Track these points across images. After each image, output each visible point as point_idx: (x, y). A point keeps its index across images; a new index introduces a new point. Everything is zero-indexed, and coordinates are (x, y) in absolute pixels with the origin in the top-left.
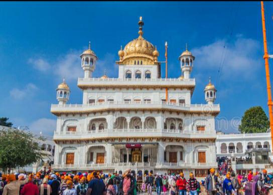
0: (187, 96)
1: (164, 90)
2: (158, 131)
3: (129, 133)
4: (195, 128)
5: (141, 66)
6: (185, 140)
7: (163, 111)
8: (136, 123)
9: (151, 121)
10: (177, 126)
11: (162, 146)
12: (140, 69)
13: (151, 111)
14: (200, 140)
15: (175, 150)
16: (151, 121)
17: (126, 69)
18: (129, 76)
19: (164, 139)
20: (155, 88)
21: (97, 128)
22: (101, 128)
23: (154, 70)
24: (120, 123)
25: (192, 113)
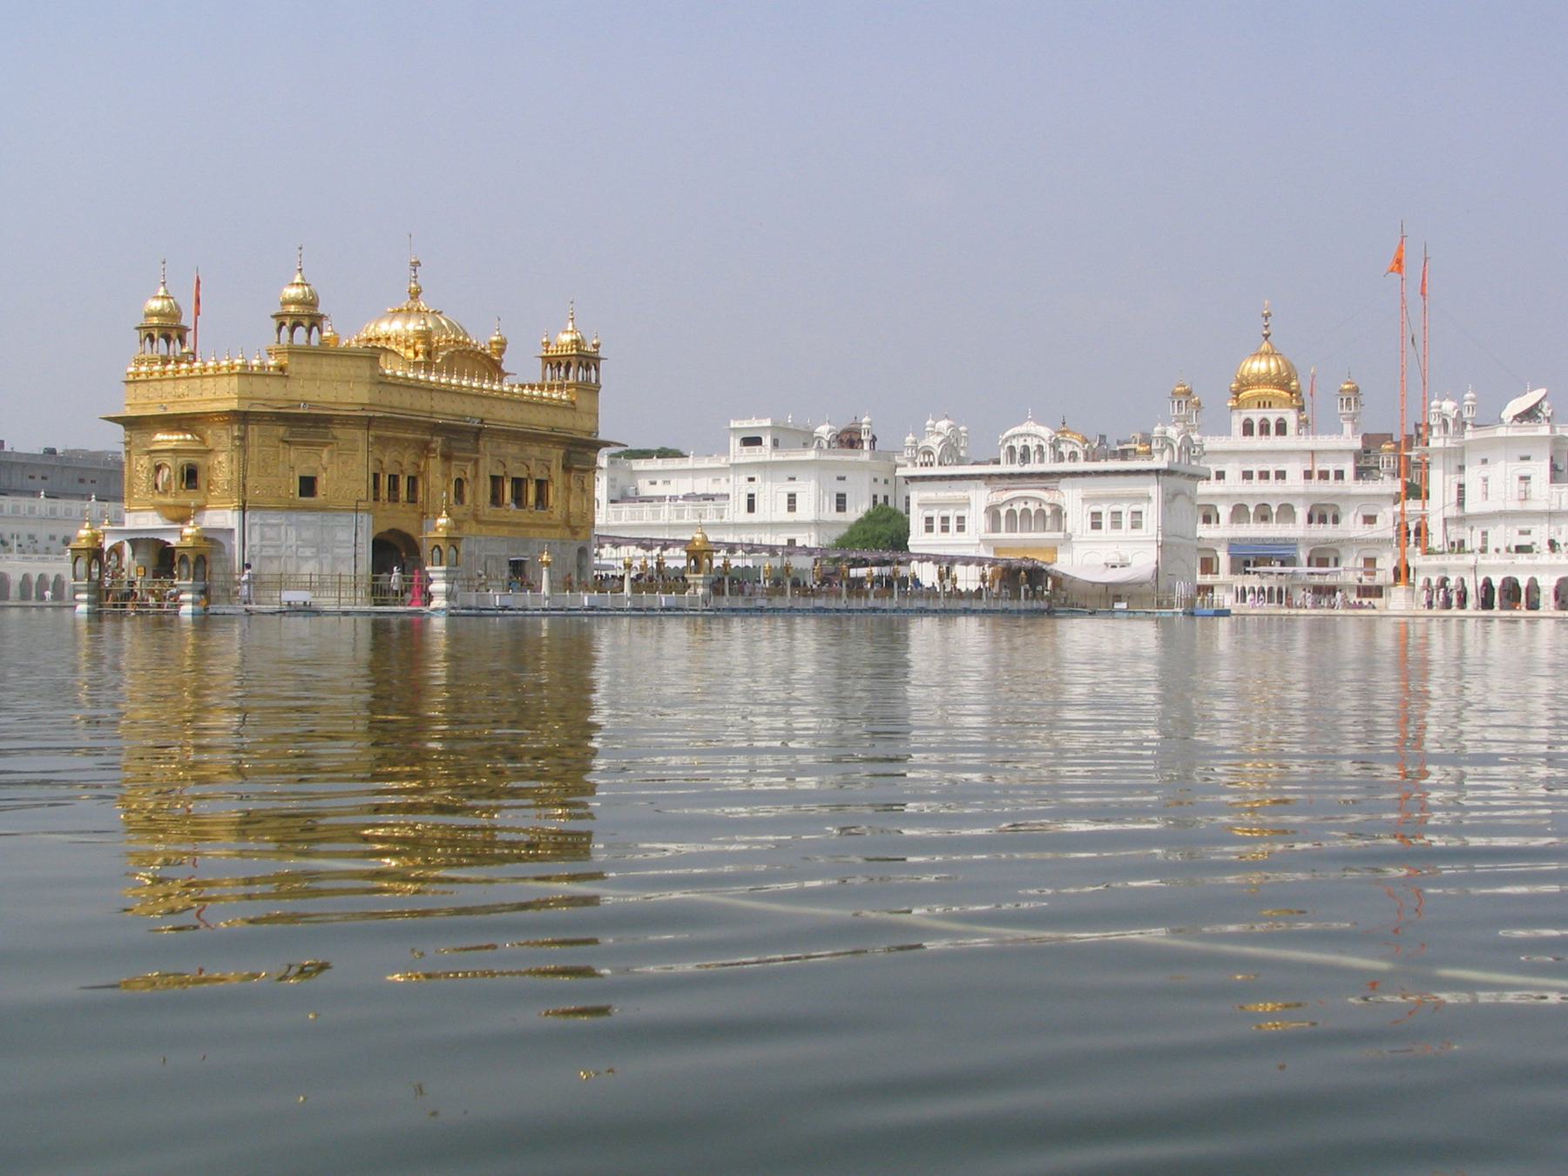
2: (1298, 529)
3: (1253, 530)
5: (1269, 410)
8: (1264, 515)
10: (1330, 518)
12: (1267, 416)
16: (1287, 512)
17: (1244, 417)
18: (1248, 429)
20: (1292, 452)
23: (1291, 418)
24: (1239, 513)
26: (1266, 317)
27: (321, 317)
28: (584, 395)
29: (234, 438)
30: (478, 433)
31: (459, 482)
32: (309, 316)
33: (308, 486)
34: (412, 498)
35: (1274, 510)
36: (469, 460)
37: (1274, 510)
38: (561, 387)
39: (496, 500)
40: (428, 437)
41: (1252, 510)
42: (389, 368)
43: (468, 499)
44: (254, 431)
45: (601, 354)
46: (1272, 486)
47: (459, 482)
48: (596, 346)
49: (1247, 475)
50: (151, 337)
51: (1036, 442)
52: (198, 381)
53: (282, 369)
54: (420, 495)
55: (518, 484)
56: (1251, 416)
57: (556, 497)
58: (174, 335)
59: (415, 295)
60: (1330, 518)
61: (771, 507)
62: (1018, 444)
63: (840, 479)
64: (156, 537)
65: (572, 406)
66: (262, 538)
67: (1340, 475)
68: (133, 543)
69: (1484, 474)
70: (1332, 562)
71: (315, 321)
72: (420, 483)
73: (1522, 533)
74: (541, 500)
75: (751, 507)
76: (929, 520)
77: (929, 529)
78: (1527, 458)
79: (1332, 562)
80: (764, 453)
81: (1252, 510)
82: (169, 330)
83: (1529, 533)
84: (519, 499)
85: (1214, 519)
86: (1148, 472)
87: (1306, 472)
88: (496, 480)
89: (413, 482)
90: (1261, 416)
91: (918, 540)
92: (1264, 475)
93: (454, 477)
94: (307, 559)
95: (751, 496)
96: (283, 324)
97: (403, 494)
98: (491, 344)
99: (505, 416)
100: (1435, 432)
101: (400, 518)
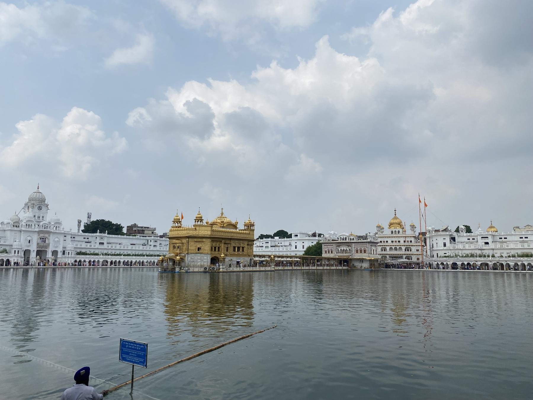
0: (413, 239)
1: (405, 238)
2: (403, 252)
4: (416, 250)
6: (412, 254)
7: (404, 245)
8: (396, 249)
9: (400, 248)
10: (409, 250)
11: (404, 256)
13: (400, 246)
14: (417, 254)
15: (409, 257)
17: (391, 230)
18: (392, 232)
19: (405, 254)
20: (401, 237)
21: (383, 250)
22: (385, 250)
23: (401, 230)
24: (391, 249)
25: (414, 246)
26: (395, 211)
27: (203, 220)
28: (251, 231)
29: (187, 241)
30: (231, 239)
31: (227, 248)
32: (200, 220)
33: (199, 249)
34: (219, 250)
35: (398, 248)
36: (229, 244)
37: (398, 248)
38: (247, 230)
39: (234, 250)
40: (221, 240)
41: (393, 248)
42: (215, 228)
43: (229, 251)
44: (190, 240)
45: (254, 224)
46: (397, 244)
47: (227, 248)
48: (254, 223)
49: (392, 242)
50: (175, 223)
51: (345, 237)
52: (181, 231)
53: (195, 229)
54: (220, 250)
55: (239, 248)
56: (393, 230)
57: (246, 250)
58: (178, 223)
59: (222, 214)
60: (409, 250)
61: (300, 248)
62: (342, 238)
63: (312, 243)
64: (172, 258)
65: (249, 234)
66: (191, 258)
67: (411, 241)
68: (170, 259)
69: (437, 242)
70: (410, 259)
71: (201, 220)
72: (220, 248)
73: (444, 254)
74: (243, 250)
75: (296, 248)
76: (326, 251)
77: (326, 253)
78: (445, 239)
79: (410, 259)
80: (299, 237)
81: (393, 248)
82: (177, 221)
83: (446, 254)
84: (238, 250)
85: (386, 250)
86: (366, 242)
87: (404, 241)
88: (234, 247)
89: (219, 248)
90: (395, 230)
91: (324, 255)
92: (396, 242)
93: (226, 246)
94: (199, 262)
95: (296, 246)
96: (196, 221)
97: (217, 250)
98: (235, 223)
99: (235, 236)
100: (427, 233)
101: (216, 254)
